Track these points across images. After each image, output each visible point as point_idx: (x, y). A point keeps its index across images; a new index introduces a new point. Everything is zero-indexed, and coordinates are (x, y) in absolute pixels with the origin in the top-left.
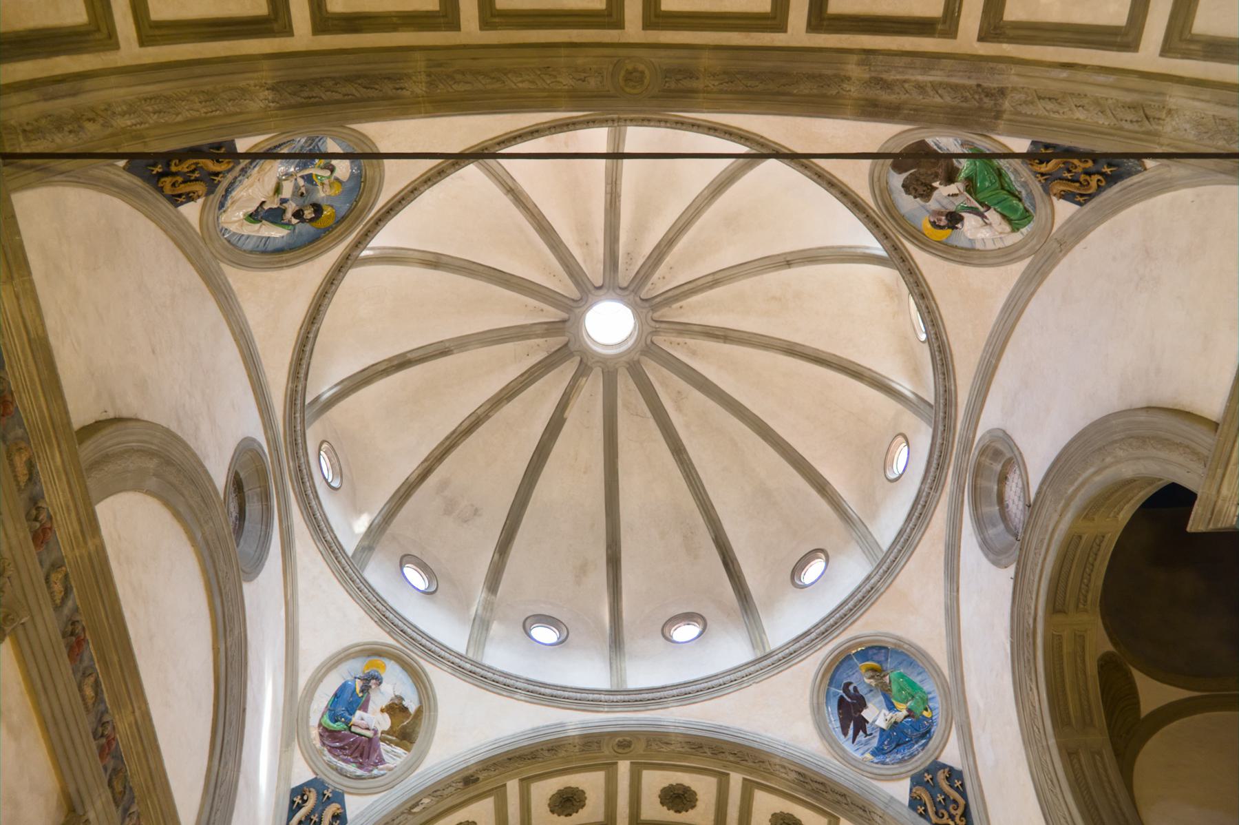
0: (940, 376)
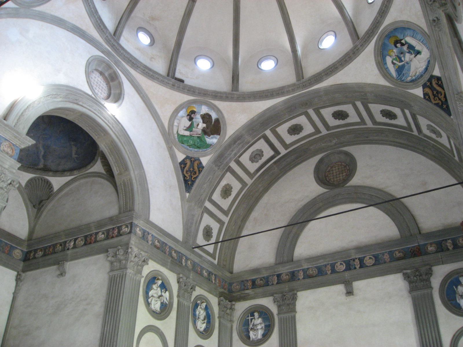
0: (143, 69)
